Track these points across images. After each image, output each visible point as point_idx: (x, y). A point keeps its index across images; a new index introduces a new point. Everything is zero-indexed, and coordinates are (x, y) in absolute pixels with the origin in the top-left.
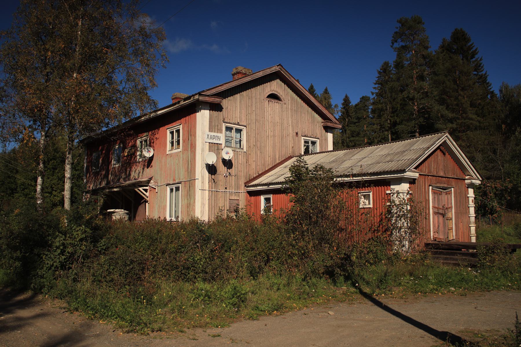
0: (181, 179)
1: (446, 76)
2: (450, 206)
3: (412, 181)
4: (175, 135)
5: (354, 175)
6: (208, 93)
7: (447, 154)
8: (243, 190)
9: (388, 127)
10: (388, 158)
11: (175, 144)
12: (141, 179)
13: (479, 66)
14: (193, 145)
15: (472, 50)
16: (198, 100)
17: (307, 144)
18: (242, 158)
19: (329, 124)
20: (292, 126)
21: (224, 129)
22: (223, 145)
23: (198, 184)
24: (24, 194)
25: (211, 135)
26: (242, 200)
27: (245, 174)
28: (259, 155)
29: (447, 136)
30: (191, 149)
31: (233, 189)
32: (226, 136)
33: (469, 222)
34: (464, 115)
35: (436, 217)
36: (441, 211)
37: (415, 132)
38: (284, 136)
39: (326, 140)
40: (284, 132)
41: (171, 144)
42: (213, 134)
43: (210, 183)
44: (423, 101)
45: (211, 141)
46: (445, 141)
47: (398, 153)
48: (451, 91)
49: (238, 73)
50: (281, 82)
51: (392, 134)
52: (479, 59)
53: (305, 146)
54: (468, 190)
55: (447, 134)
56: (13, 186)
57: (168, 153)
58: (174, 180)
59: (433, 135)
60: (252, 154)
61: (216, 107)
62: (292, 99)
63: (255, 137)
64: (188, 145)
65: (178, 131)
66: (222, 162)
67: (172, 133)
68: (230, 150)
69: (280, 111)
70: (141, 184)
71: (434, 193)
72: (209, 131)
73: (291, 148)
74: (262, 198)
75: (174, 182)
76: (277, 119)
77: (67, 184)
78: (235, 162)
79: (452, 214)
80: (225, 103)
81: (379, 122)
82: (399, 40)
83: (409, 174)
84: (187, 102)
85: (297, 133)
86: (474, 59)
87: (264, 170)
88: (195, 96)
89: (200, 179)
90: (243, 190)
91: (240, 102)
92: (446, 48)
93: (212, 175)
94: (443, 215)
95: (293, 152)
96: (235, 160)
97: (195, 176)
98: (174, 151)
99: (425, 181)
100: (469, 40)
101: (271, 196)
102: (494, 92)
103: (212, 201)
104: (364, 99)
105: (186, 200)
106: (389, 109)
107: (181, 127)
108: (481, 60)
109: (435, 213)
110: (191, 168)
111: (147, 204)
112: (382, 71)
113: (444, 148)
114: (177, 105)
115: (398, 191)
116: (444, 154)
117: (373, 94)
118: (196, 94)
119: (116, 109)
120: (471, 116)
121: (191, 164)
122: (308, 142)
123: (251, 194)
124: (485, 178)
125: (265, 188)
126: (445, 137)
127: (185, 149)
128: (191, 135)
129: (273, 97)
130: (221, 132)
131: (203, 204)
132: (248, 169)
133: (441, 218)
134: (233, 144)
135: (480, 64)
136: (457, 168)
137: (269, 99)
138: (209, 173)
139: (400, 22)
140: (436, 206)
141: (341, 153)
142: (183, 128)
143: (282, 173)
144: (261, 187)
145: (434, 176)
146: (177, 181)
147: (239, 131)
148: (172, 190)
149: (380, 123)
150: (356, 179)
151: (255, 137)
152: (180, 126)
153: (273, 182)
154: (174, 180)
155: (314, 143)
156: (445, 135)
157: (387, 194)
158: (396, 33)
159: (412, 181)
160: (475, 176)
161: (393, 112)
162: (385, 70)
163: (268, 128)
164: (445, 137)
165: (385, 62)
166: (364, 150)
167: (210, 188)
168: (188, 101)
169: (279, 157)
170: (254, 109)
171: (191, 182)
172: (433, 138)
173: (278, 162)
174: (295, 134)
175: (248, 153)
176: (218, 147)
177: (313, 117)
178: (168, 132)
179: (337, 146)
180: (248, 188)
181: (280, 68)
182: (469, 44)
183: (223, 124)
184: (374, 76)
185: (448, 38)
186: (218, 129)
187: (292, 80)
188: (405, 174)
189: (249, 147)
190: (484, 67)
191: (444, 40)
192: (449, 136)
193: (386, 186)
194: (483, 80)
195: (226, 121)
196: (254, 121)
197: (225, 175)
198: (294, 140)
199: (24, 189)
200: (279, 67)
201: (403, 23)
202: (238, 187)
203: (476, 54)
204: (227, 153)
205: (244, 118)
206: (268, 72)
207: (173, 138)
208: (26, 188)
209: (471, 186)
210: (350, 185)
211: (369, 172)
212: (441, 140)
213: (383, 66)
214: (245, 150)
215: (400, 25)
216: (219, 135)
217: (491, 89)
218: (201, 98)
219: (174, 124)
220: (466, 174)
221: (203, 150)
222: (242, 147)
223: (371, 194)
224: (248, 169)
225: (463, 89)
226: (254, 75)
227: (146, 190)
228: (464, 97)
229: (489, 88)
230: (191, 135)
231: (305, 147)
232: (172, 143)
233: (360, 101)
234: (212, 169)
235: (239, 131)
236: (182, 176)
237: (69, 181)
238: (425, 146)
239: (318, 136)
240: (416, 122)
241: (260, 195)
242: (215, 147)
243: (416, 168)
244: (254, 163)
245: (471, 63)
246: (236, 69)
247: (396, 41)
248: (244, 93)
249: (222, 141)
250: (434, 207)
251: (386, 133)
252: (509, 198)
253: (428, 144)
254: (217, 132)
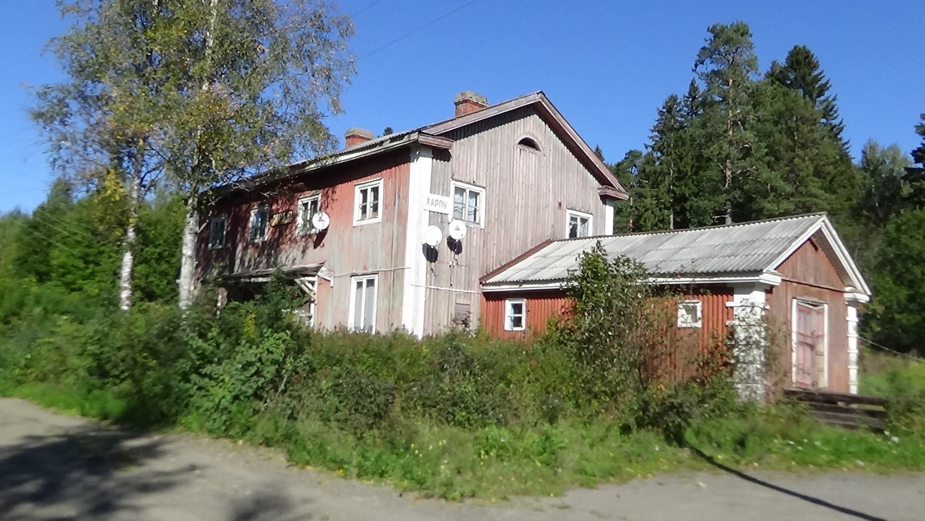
0: (378, 267)
1: (776, 123)
2: (821, 333)
3: (769, 290)
4: (370, 195)
5: (663, 275)
6: (433, 131)
7: (820, 249)
8: (476, 289)
9: (669, 202)
10: (728, 251)
11: (369, 210)
12: (301, 263)
13: (831, 110)
14: (403, 212)
15: (819, 83)
16: (416, 142)
17: (573, 223)
18: (476, 239)
19: (610, 192)
20: (554, 193)
21: (452, 190)
22: (450, 217)
23: (409, 277)
24: (63, 282)
26: (475, 304)
27: (481, 265)
28: (503, 235)
29: (823, 221)
30: (398, 220)
31: (463, 287)
32: (455, 202)
33: (847, 362)
34: (802, 189)
35: (801, 349)
36: (809, 341)
37: (725, 213)
39: (603, 216)
41: (361, 211)
42: (435, 197)
43: (428, 276)
44: (742, 163)
45: (433, 209)
46: (820, 230)
47: (744, 243)
48: (782, 149)
49: (466, 101)
50: (540, 120)
51: (676, 214)
52: (830, 99)
53: (570, 224)
54: (847, 309)
55: (824, 218)
56: (43, 268)
57: (355, 224)
58: (365, 268)
59: (800, 218)
60: (492, 232)
61: (442, 154)
62: (556, 147)
63: (498, 206)
64: (394, 210)
65: (375, 190)
66: (448, 243)
67: (364, 192)
68: (462, 225)
70: (304, 273)
71: (800, 310)
72: (432, 191)
73: (550, 225)
74: (508, 304)
75: (366, 272)
76: (532, 179)
77: (187, 266)
78: (467, 244)
79: (824, 346)
80: (457, 148)
81: (655, 194)
82: (708, 61)
83: (768, 278)
84: (395, 143)
86: (822, 98)
87: (509, 261)
88: (412, 135)
89: (413, 268)
90: (476, 291)
91: (479, 148)
92: (777, 77)
93: (431, 262)
94: (812, 347)
95: (554, 234)
96: (467, 240)
97: (403, 265)
98: (367, 222)
99: (787, 290)
100: (815, 66)
101: (523, 302)
102: (849, 154)
103: (429, 305)
104: (632, 155)
105: (386, 302)
106: (674, 173)
107: (381, 184)
108: (834, 100)
109: (801, 343)
110: (398, 250)
111: (312, 305)
112: (665, 110)
113: (817, 242)
114: (378, 148)
115: (753, 303)
116: (816, 249)
117: (646, 147)
118: (413, 132)
119: (272, 149)
120: (814, 190)
121: (398, 244)
122: (576, 219)
123: (489, 296)
124: (875, 291)
125: (515, 288)
126: (820, 223)
127: (388, 219)
128: (399, 196)
129: (527, 143)
130: (448, 195)
131: (416, 309)
132: (485, 256)
133: (808, 350)
134: (465, 215)
135: (833, 107)
136: (833, 273)
137: (521, 146)
138: (428, 260)
139: (712, 30)
140: (802, 332)
141: (639, 239)
142: (385, 186)
143: (542, 266)
144: (508, 286)
145: (799, 283)
146: (370, 271)
147: (474, 195)
148: (360, 284)
149: (657, 196)
150: (698, 280)
151: (498, 206)
152: (378, 181)
153: (530, 279)
154: (365, 268)
155: (584, 221)
156: (822, 219)
157: (727, 307)
158: (704, 48)
159: (769, 289)
160: (859, 288)
161: (678, 179)
162: (670, 108)
164: (820, 223)
165: (672, 96)
166: (677, 237)
167: (428, 283)
168: (399, 142)
169: (532, 240)
170: (498, 161)
171: (396, 274)
172: (801, 222)
173: (530, 247)
174: (557, 205)
175: (486, 231)
176: (442, 218)
177: (585, 179)
178: (357, 190)
179: (619, 230)
180: (485, 287)
181: (541, 98)
182: (815, 73)
183: (453, 182)
184: (652, 119)
185: (782, 62)
186: (443, 190)
187: (557, 117)
188: (761, 276)
189: (488, 221)
190: (838, 112)
191: (774, 63)
192: (827, 221)
193: (727, 295)
194: (834, 132)
195: (454, 177)
197: (451, 264)
198: (555, 214)
199: (64, 275)
200: (540, 95)
201: (717, 33)
202: (469, 285)
203: (828, 89)
205: (482, 174)
206: (523, 103)
207: (365, 200)
208: (69, 273)
209: (854, 303)
210: (675, 289)
211: (699, 272)
212: (814, 225)
213: (667, 103)
214: (482, 226)
215: (711, 36)
216: (444, 199)
217: (847, 148)
218: (422, 139)
219: (368, 179)
220: (846, 283)
221: (419, 223)
222: (477, 221)
223: (699, 306)
224: (485, 256)
225: (803, 146)
226: (502, 106)
227: (313, 283)
228: (804, 160)
229: (846, 146)
230: (399, 196)
231: (571, 227)
232: (364, 209)
233: (626, 158)
234: (431, 254)
235: (474, 195)
236: (380, 261)
237: (189, 261)
238: (791, 234)
239: (592, 210)
240: (728, 197)
241: (505, 299)
242: (437, 219)
243: (775, 269)
245: (817, 103)
246: (463, 94)
247: (702, 63)
248: (485, 134)
249: (449, 210)
250: (799, 333)
251: (666, 212)
252: (878, 329)
253: (794, 232)
254: (443, 195)
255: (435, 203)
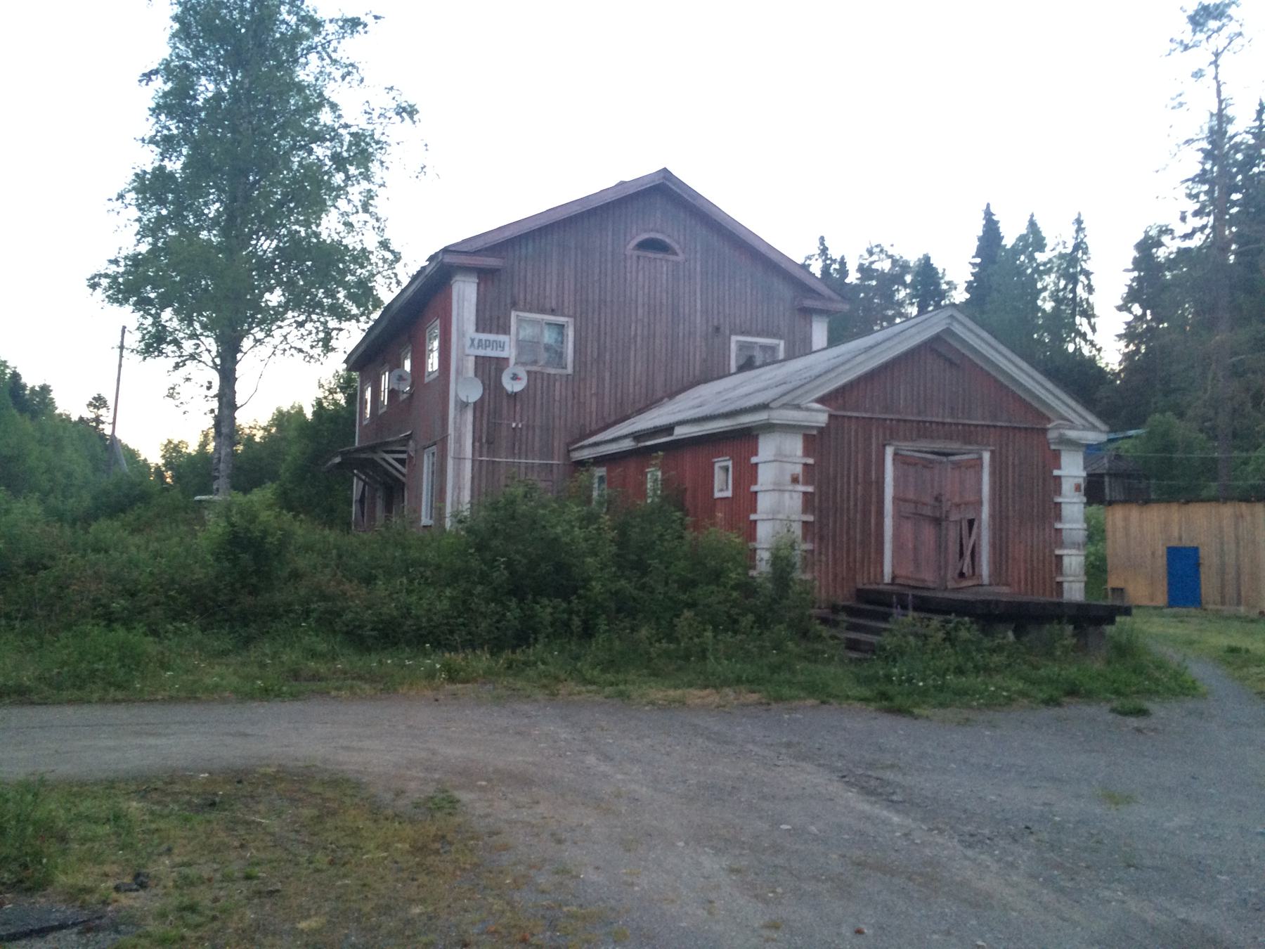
25: (480, 340)
38: (681, 335)
40: (681, 326)
42: (484, 336)
43: (477, 444)
45: (481, 352)
69: (670, 280)
72: (477, 330)
85: (717, 329)
114: (422, 277)
151: (599, 341)
163: (633, 318)
167: (477, 454)
186: (498, 326)
196: (596, 305)
204: (515, 377)
214: (570, 370)
216: (502, 338)
224: (575, 413)
244: (594, 400)
254: (497, 333)
255: (488, 344)
